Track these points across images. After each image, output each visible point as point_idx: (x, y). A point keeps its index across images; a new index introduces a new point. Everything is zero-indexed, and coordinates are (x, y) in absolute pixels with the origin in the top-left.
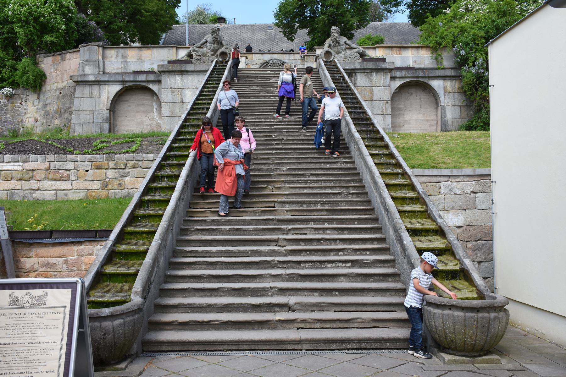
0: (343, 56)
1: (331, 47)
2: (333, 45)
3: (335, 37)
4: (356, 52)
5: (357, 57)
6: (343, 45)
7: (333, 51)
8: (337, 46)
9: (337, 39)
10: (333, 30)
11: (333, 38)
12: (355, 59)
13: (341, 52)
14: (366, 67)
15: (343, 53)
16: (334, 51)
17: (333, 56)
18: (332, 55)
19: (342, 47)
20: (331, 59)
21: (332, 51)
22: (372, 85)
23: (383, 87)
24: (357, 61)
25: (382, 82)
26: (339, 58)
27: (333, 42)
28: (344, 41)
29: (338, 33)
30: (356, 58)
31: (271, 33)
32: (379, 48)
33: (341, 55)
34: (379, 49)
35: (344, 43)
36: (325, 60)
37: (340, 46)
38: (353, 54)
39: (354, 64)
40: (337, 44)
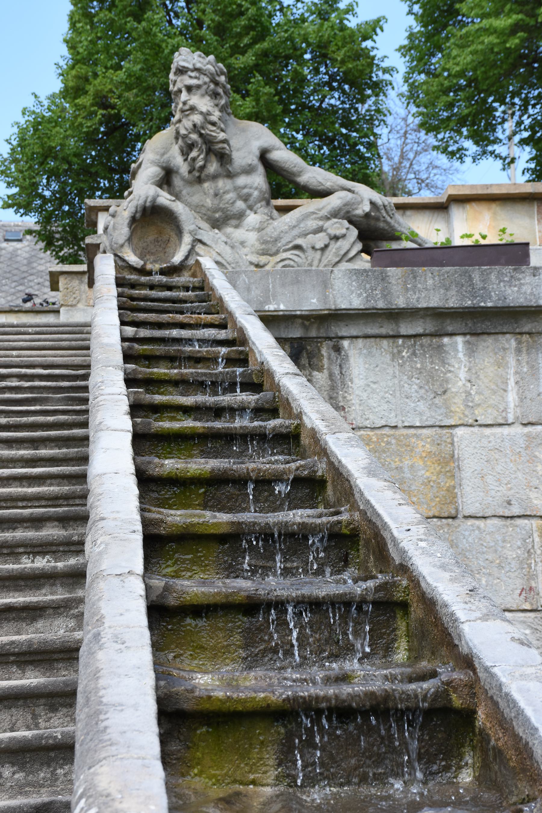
0: (252, 237)
1: (177, 182)
2: (183, 168)
3: (197, 118)
4: (335, 214)
5: (344, 245)
6: (249, 170)
7: (187, 204)
8: (214, 177)
9: (210, 130)
10: (182, 71)
11: (187, 123)
12: (331, 255)
13: (240, 216)
14: (401, 302)
15: (252, 219)
16: (196, 208)
17: (187, 239)
18: (179, 232)
19: (242, 180)
20: (177, 259)
21: (178, 208)
22: (449, 413)
23: (518, 429)
24: (345, 266)
25: (512, 397)
26: (227, 251)
27: (185, 152)
28: (255, 146)
29: (215, 95)
30: (334, 246)
31: (14, 254)
32: (474, 204)
33: (238, 234)
34: (471, 209)
35: (253, 159)
36: (133, 259)
37: (230, 175)
38: (312, 224)
39: (325, 284)
40: (213, 167)
